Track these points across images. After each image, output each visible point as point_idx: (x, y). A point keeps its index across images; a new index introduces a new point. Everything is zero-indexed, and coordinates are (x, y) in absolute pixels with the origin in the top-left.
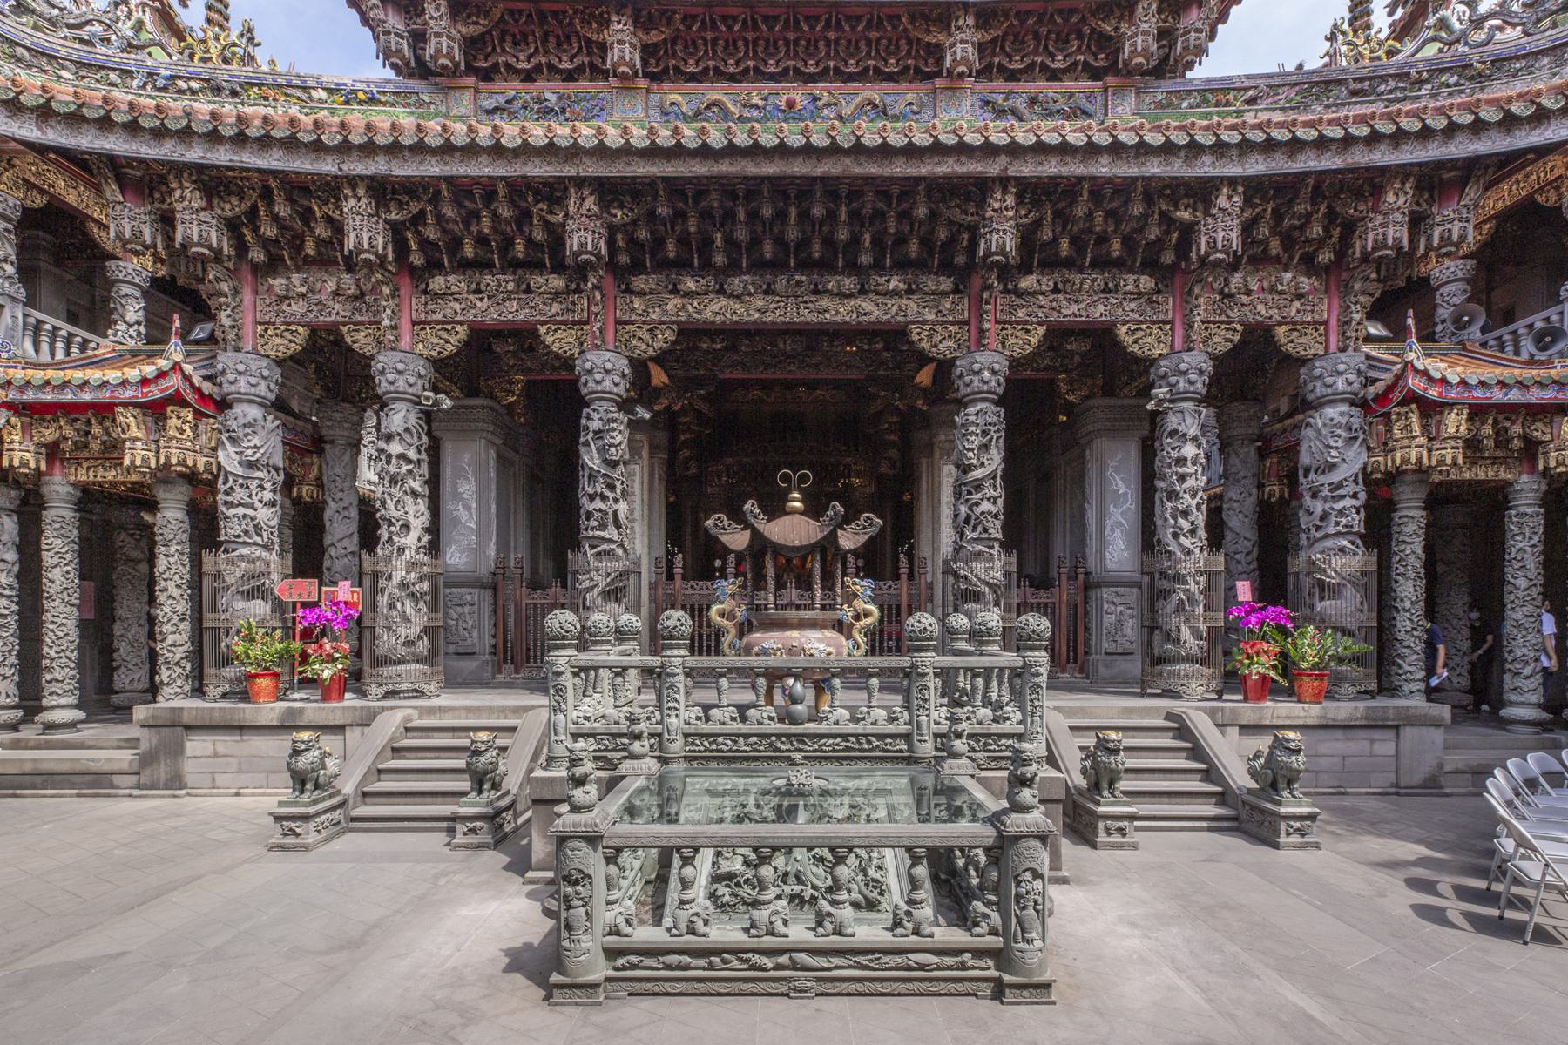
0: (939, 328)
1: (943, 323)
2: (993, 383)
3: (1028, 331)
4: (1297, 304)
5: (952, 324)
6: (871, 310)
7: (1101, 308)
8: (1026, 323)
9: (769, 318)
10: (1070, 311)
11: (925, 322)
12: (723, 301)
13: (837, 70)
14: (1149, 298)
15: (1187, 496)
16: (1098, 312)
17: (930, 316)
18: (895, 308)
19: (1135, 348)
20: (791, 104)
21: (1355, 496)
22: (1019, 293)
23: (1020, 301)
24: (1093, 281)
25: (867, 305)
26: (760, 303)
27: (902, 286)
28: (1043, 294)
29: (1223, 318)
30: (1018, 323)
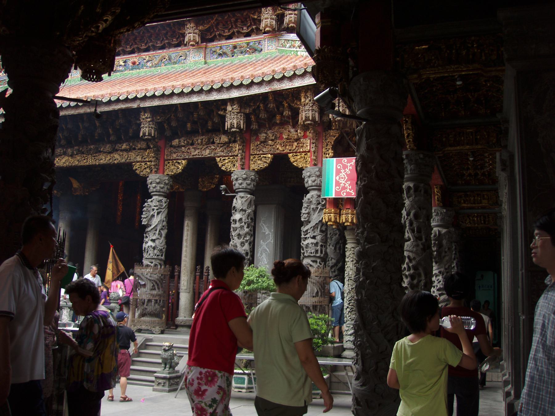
0: (143, 164)
1: (144, 162)
2: (158, 188)
3: (179, 163)
4: (295, 144)
5: (149, 161)
6: (118, 158)
7: (208, 151)
8: (178, 159)
9: (82, 164)
10: (195, 153)
11: (138, 162)
12: (66, 158)
13: (153, 46)
14: (226, 145)
15: (236, 238)
16: (206, 153)
17: (139, 159)
18: (126, 157)
19: (223, 168)
20: (134, 63)
21: (314, 237)
22: (174, 147)
23: (174, 150)
24: (202, 140)
25: (116, 156)
26: (78, 158)
27: (128, 147)
28: (184, 146)
29: (261, 152)
30: (175, 160)
